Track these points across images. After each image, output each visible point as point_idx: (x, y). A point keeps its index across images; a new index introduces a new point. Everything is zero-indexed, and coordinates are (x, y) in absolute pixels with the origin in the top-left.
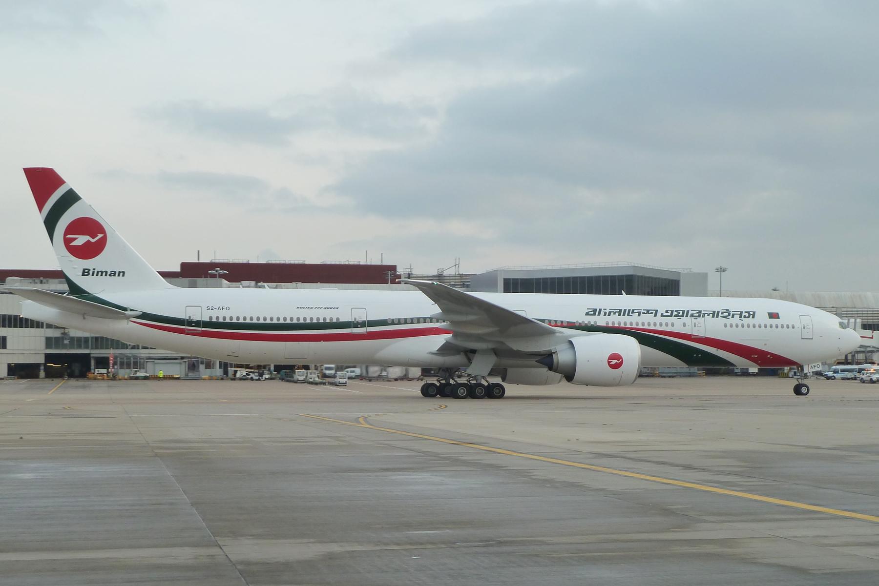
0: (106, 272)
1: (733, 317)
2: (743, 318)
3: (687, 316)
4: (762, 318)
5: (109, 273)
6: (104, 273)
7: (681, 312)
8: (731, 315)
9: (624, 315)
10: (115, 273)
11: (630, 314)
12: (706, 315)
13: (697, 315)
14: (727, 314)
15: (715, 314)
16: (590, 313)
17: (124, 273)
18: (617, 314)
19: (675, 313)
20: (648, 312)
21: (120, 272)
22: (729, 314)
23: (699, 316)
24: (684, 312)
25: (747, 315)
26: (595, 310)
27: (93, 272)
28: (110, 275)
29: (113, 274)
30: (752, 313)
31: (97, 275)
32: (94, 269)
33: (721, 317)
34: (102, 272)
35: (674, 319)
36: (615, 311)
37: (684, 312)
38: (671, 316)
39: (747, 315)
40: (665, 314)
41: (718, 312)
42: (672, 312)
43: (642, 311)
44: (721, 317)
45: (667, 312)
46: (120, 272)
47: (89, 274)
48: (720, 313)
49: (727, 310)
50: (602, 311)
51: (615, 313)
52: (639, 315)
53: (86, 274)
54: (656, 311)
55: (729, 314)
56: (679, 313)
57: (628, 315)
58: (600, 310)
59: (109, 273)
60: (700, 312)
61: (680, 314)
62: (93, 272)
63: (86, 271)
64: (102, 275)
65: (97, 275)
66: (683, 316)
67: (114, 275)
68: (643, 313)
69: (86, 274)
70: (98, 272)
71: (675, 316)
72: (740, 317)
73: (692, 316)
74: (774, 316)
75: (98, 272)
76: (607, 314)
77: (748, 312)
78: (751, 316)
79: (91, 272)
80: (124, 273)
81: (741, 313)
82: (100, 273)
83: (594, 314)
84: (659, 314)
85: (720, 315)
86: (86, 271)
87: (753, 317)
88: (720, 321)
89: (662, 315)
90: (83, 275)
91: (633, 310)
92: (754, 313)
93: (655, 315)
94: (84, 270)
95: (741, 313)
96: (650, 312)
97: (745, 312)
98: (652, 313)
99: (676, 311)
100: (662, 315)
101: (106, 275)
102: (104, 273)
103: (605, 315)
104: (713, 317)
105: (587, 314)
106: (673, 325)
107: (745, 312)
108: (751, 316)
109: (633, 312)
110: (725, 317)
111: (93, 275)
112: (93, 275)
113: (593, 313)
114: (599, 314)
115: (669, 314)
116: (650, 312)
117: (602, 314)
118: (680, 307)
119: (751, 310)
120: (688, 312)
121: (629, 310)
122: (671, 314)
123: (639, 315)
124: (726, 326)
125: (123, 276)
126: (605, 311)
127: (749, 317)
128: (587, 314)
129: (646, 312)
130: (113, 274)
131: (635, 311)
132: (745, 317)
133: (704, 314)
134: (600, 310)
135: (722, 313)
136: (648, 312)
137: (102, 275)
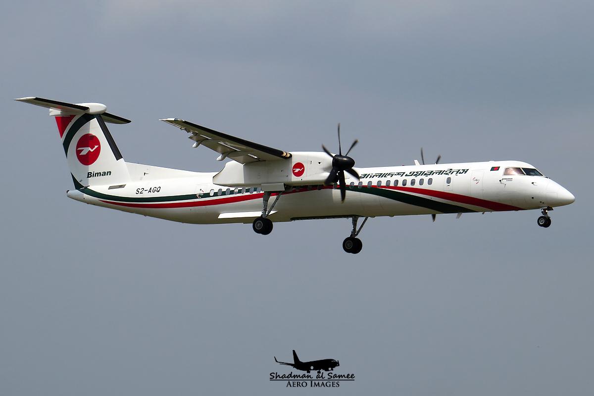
0: (100, 173)
10: (105, 172)
17: (110, 172)
19: (415, 173)
21: (108, 172)
28: (102, 175)
29: (104, 174)
46: (108, 172)
66: (419, 175)
67: (105, 175)
75: (96, 174)
79: (92, 174)
80: (110, 172)
93: (402, 176)
94: (89, 173)
103: (371, 176)
109: (389, 175)
117: (369, 176)
125: (110, 174)
130: (104, 174)
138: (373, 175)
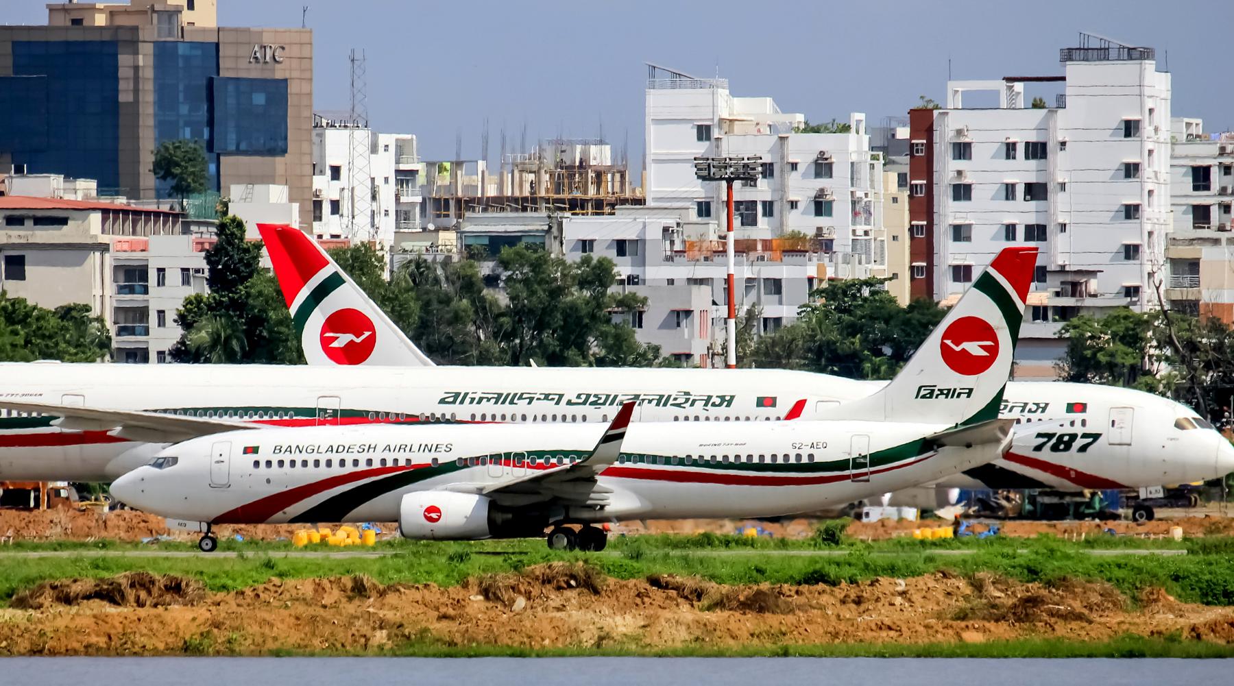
1: (692, 405)
7: (604, 398)
8: (690, 402)
9: (503, 403)
11: (515, 401)
14: (684, 400)
16: (446, 400)
19: (592, 399)
20: (547, 397)
22: (687, 400)
24: (608, 396)
25: (718, 401)
26: (457, 395)
30: (727, 398)
33: (671, 405)
36: (490, 396)
38: (584, 403)
39: (718, 401)
40: (574, 400)
43: (536, 396)
44: (671, 405)
45: (579, 396)
48: (672, 398)
49: (687, 393)
51: (489, 400)
52: (529, 403)
54: (561, 396)
55: (687, 400)
56: (600, 398)
57: (512, 402)
61: (601, 401)
66: (604, 404)
68: (538, 399)
71: (590, 404)
72: (706, 405)
77: (722, 398)
83: (454, 402)
84: (564, 400)
85: (671, 402)
87: (728, 405)
89: (569, 403)
91: (522, 394)
92: (732, 397)
93: (557, 403)
96: (550, 397)
98: (553, 399)
99: (596, 396)
100: (569, 403)
103: (471, 402)
105: (442, 401)
109: (521, 398)
110: (679, 405)
114: (462, 402)
115: (581, 401)
116: (550, 397)
117: (468, 400)
119: (728, 393)
120: (616, 397)
123: (529, 403)
126: (473, 396)
127: (720, 405)
128: (442, 401)
129: (542, 397)
131: (524, 396)
134: (466, 394)
135: (675, 399)
136: (547, 397)
138: (477, 397)
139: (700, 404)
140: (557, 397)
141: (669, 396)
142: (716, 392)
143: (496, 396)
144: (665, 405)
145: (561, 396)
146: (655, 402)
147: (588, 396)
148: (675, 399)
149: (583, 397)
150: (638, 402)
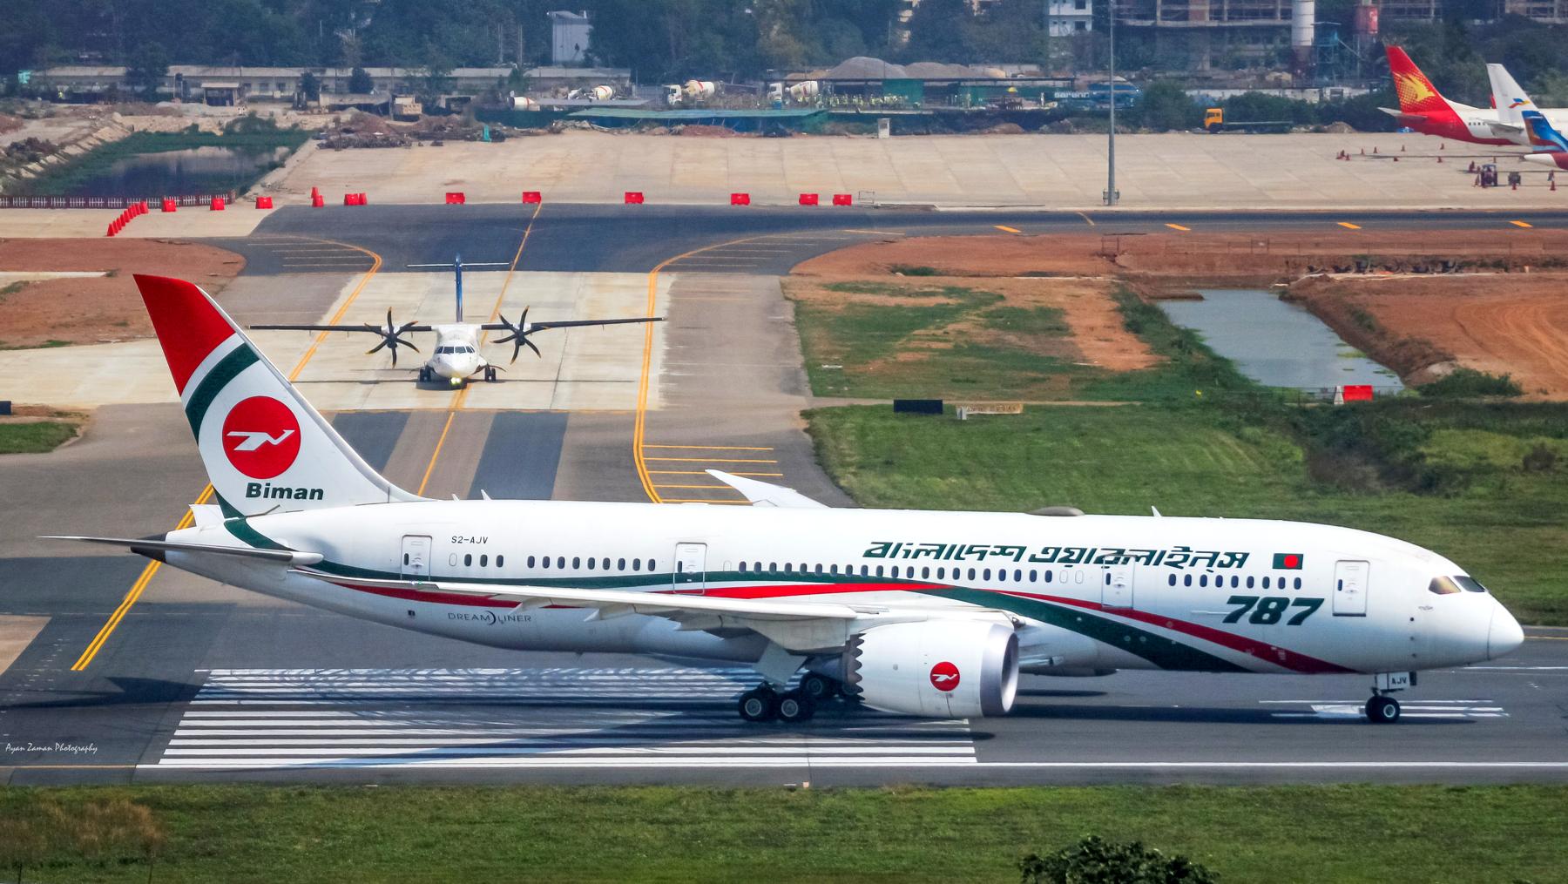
0: (290, 491)
1: (1193, 564)
2: (1215, 567)
3: (1087, 561)
4: (1260, 566)
5: (294, 493)
6: (286, 493)
7: (1077, 552)
9: (947, 557)
11: (962, 555)
12: (1132, 560)
13: (1111, 558)
14: (1181, 558)
15: (1152, 558)
18: (933, 554)
19: (1062, 554)
20: (1003, 551)
22: (1186, 557)
23: (1116, 561)
25: (1227, 560)
26: (887, 546)
27: (267, 490)
28: (297, 497)
30: (1239, 556)
31: (274, 496)
32: (268, 484)
33: (1166, 563)
34: (282, 491)
35: (1056, 568)
36: (929, 548)
37: (1083, 551)
38: (1052, 560)
39: (1227, 560)
41: (1163, 553)
42: (1057, 550)
43: (991, 549)
44: (1166, 563)
45: (1045, 551)
47: (258, 494)
49: (1186, 549)
50: (902, 548)
51: (928, 553)
52: (981, 558)
53: (254, 493)
54: (1022, 550)
55: (1186, 557)
56: (1072, 554)
57: (958, 557)
58: (899, 546)
59: (294, 493)
60: (1121, 552)
62: (267, 490)
63: (255, 488)
64: (281, 496)
65: (274, 496)
66: (1077, 561)
68: (993, 553)
69: (254, 493)
70: (275, 490)
71: (1060, 561)
72: (1210, 565)
73: (1100, 560)
74: (1293, 561)
76: (911, 555)
77: (1232, 556)
78: (1236, 563)
79: (262, 491)
81: (1216, 555)
82: (278, 492)
83: (883, 555)
84: (1026, 555)
85: (1165, 559)
86: (255, 488)
87: (1240, 566)
88: (1165, 571)
89: (1033, 559)
90: (249, 495)
91: (972, 547)
92: (1246, 556)
93: (1017, 559)
95: (1216, 555)
96: (1007, 551)
97: (1227, 554)
98: (1011, 554)
99: (1067, 550)
100: (1033, 559)
101: (289, 497)
102: (286, 493)
103: (907, 553)
104: (1147, 563)
105: (869, 554)
106: (1049, 576)
107: (1227, 554)
108: (1236, 563)
109: (970, 551)
110: (1175, 564)
111: (266, 496)
112: (266, 496)
113: (880, 551)
114: (893, 556)
115: (1048, 556)
116: (1007, 551)
117: (901, 553)
118: (1076, 542)
119: (1239, 549)
120: (1094, 551)
121: (963, 547)
122: (1051, 555)
123: (981, 558)
124: (1172, 580)
126: (908, 548)
127: (1229, 565)
128: (869, 554)
129: (998, 550)
130: (302, 494)
131: (975, 549)
132: (1221, 565)
133: (1127, 560)
134: (899, 546)
135: (1171, 556)
136: (1003, 551)
137: (281, 496)
138: (913, 549)
139: (1201, 568)
140: (1016, 551)
141: (1163, 553)
142: (1223, 548)
143: (937, 548)
144: (1157, 563)
145: (1022, 550)
146: (1143, 560)
147: (1057, 550)
148: (1171, 556)
149: (1051, 552)
150: (1122, 559)
